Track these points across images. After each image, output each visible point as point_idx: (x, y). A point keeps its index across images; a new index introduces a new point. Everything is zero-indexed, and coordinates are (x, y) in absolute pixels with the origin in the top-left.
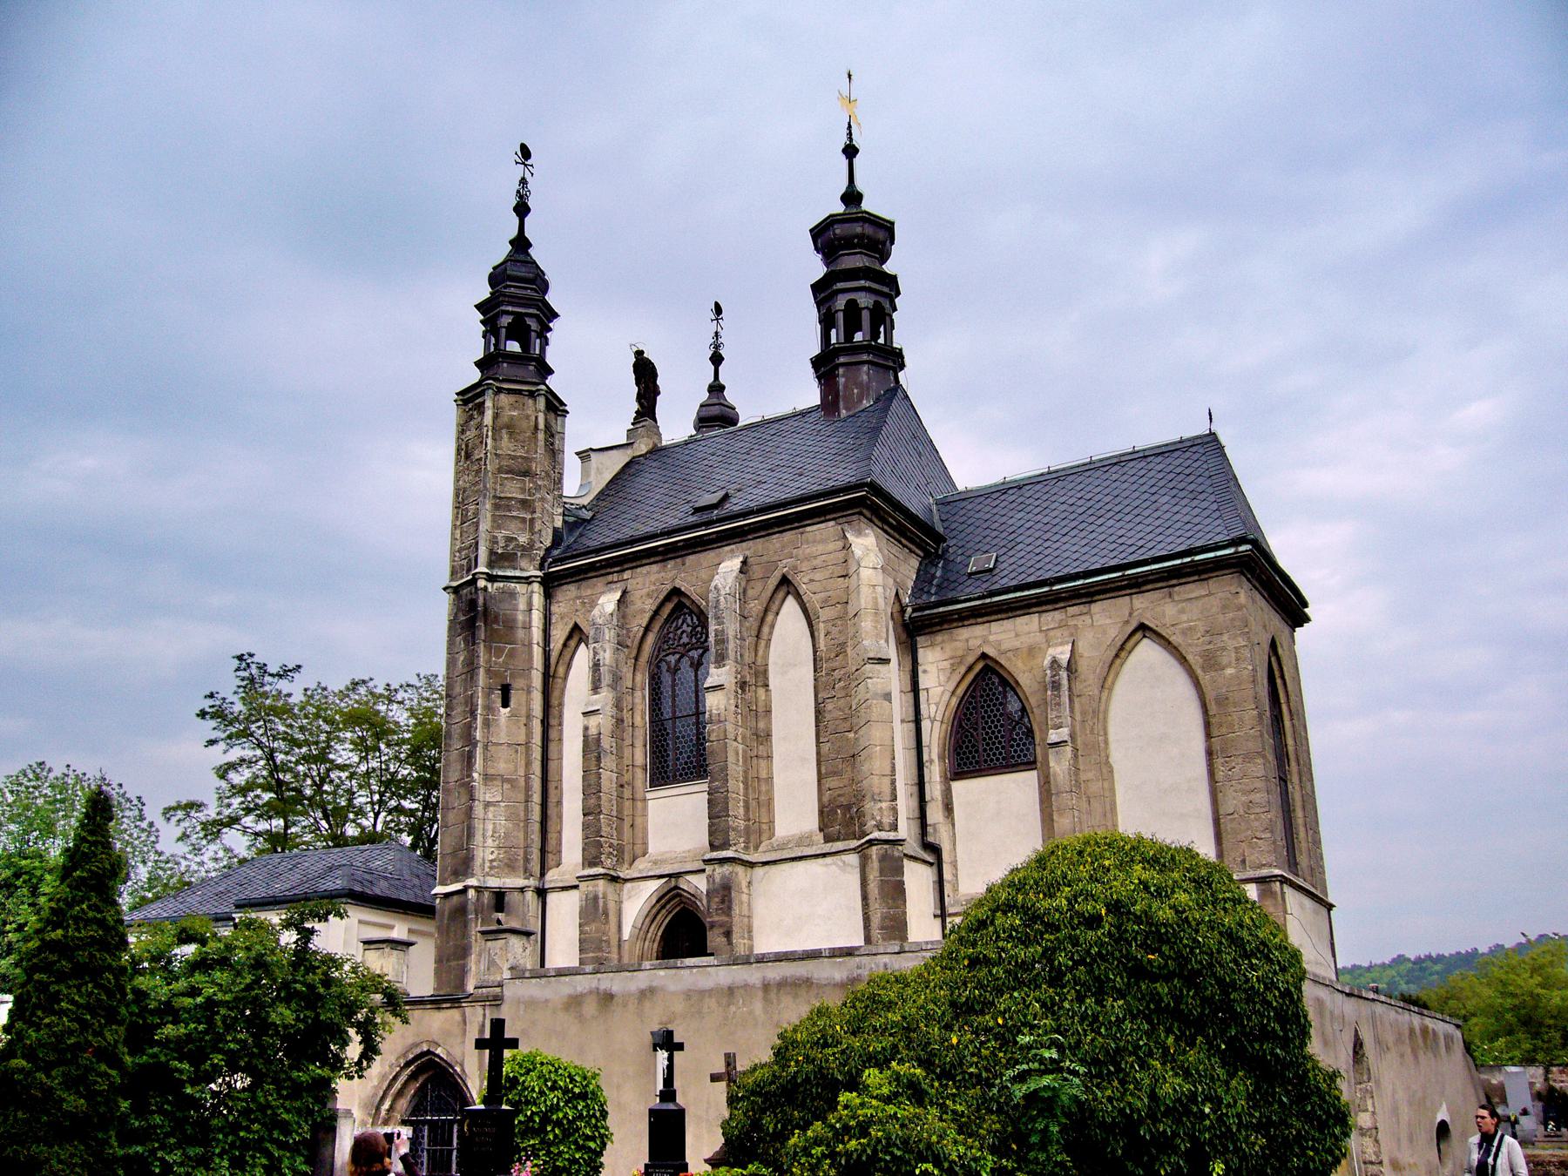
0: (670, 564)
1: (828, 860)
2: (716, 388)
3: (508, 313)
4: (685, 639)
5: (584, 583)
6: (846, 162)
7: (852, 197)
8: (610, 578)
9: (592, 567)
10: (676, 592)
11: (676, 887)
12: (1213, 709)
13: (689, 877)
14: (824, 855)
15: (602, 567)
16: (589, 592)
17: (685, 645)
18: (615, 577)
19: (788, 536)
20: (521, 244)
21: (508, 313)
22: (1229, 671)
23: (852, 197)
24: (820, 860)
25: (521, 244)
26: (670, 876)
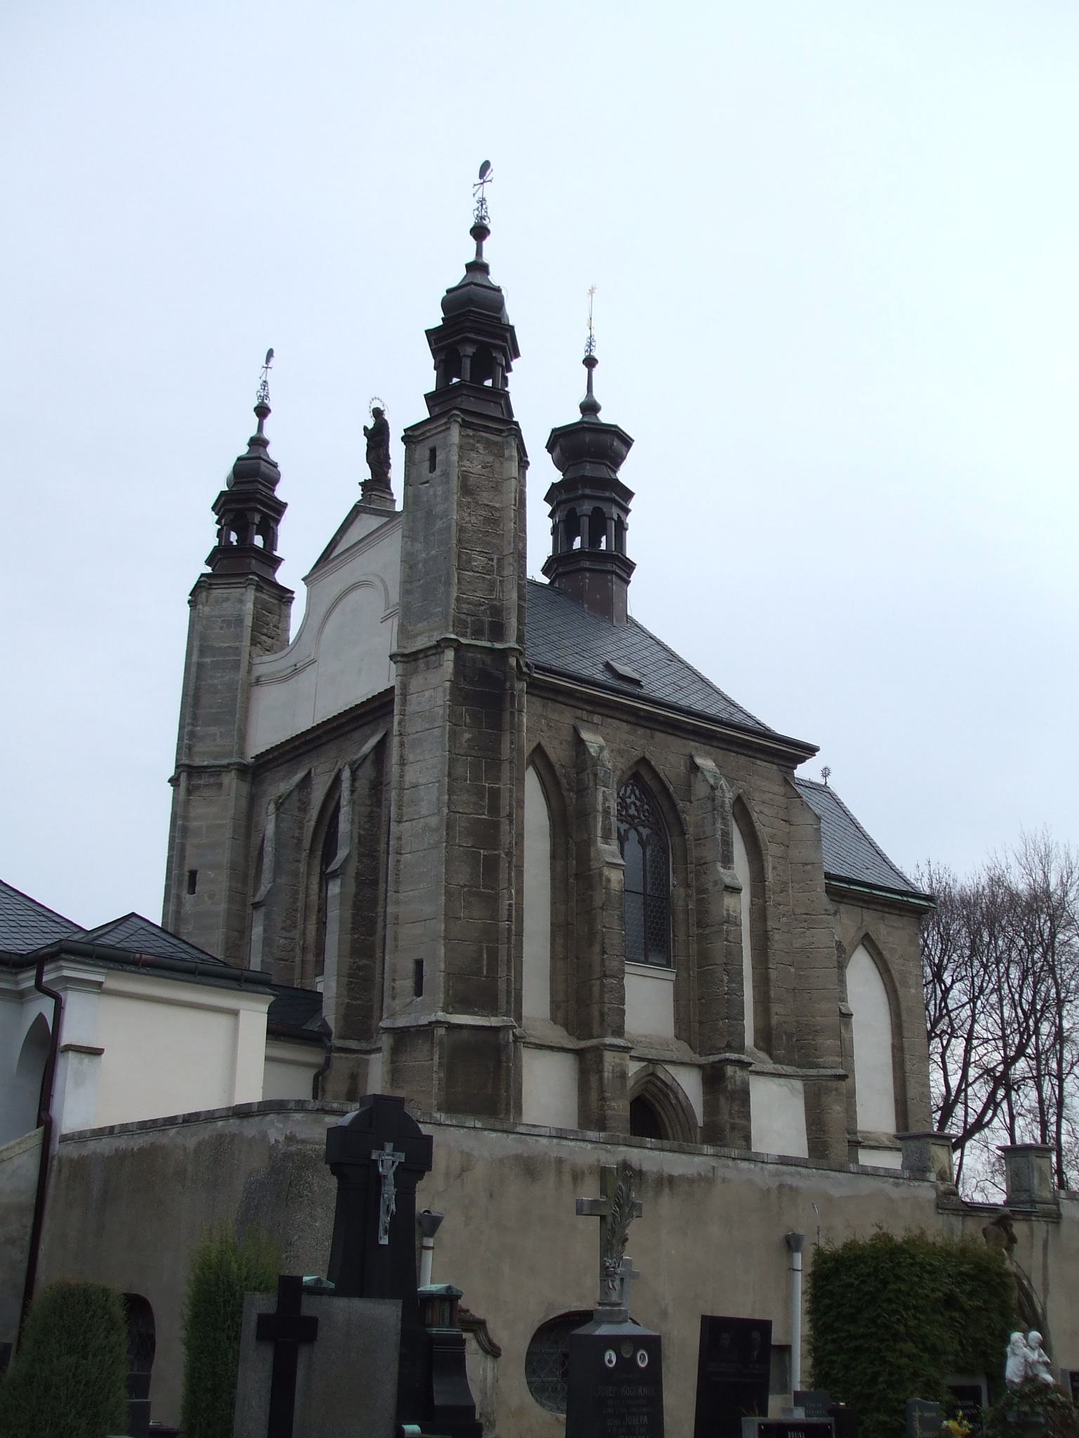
0: (641, 731)
1: (782, 1081)
2: (258, 443)
3: (473, 341)
4: (632, 811)
5: (550, 704)
6: (586, 370)
7: (590, 407)
8: (579, 713)
9: (570, 693)
10: (643, 761)
11: (653, 1074)
12: (904, 1016)
13: (667, 1067)
14: (780, 1076)
15: (579, 699)
16: (555, 717)
17: (633, 817)
18: (585, 715)
19: (743, 759)
20: (477, 267)
21: (473, 341)
22: (913, 991)
23: (590, 407)
24: (776, 1080)
25: (477, 267)
26: (650, 1061)
